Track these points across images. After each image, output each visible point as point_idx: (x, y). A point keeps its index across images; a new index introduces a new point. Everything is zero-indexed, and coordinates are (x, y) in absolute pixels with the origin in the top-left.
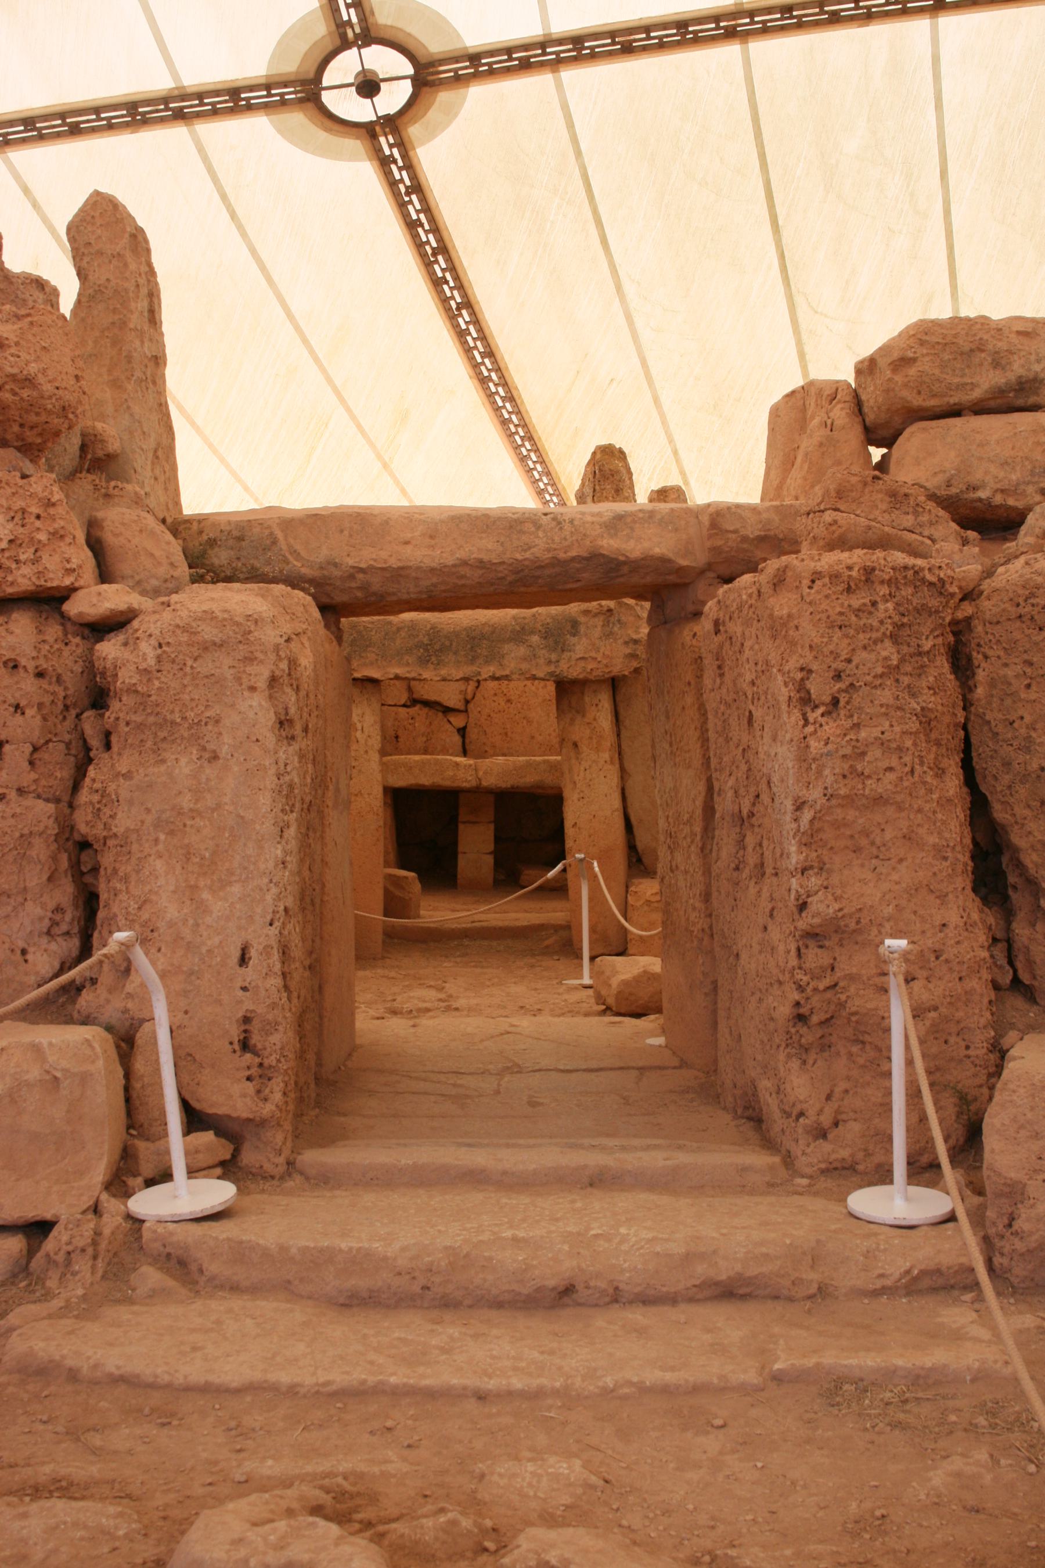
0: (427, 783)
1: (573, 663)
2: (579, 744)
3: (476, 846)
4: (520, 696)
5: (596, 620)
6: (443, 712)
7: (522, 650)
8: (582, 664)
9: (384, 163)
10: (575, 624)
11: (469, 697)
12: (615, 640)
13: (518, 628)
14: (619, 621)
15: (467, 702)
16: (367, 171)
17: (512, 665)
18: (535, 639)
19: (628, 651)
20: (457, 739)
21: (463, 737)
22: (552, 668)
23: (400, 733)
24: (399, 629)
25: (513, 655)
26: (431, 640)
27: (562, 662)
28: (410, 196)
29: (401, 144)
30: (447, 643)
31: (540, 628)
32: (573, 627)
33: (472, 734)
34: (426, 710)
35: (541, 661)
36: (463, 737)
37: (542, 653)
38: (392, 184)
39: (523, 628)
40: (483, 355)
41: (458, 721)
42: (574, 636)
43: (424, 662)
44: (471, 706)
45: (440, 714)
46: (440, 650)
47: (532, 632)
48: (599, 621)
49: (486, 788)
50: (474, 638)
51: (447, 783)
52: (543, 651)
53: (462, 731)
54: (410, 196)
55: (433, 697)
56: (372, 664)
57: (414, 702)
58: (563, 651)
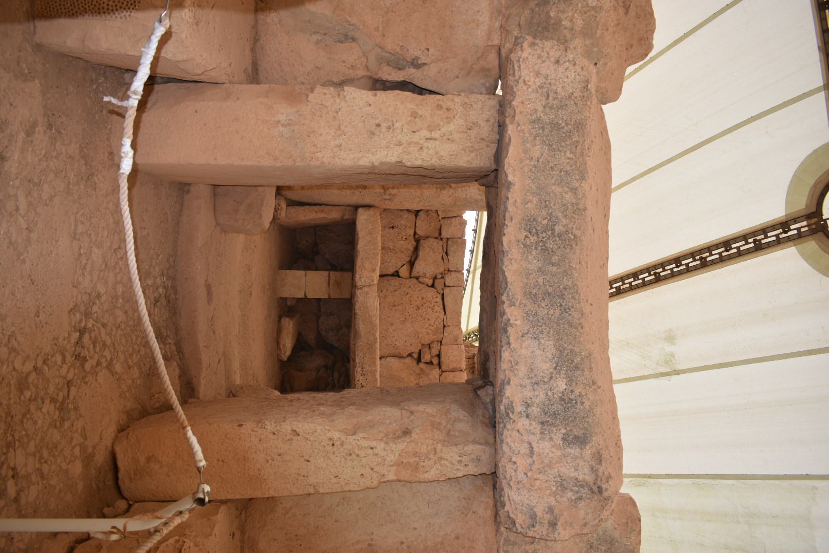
0: (359, 246)
1: (525, 438)
2: (407, 439)
3: (310, 284)
4: (421, 316)
5: (587, 470)
6: (410, 261)
7: (545, 367)
8: (524, 449)
9: (784, 225)
10: (581, 441)
11: (421, 279)
12: (554, 494)
13: (577, 360)
14: (580, 498)
15: (417, 278)
16: (776, 211)
17: (524, 352)
18: (561, 385)
19: (539, 511)
20: (391, 270)
21: (392, 275)
22: (519, 408)
23: (395, 229)
24: (574, 190)
25: (538, 352)
26: (559, 236)
27: (526, 422)
28: (757, 242)
29: (800, 235)
30: (555, 259)
31: (577, 392)
32: (577, 438)
33: (395, 281)
34: (412, 249)
35: (528, 393)
36: (392, 275)
37: (540, 396)
38: (764, 231)
39: (577, 367)
40: (618, 289)
41: (404, 272)
42: (564, 439)
43: (530, 224)
44: (414, 281)
45: (409, 259)
46: (545, 249)
47: (570, 381)
48: (584, 474)
49: (355, 293)
50: (562, 296)
51: (359, 262)
52: (542, 396)
53: (396, 274)
54: (757, 242)
55: (421, 253)
56: (526, 151)
57: (418, 241)
58: (542, 423)
